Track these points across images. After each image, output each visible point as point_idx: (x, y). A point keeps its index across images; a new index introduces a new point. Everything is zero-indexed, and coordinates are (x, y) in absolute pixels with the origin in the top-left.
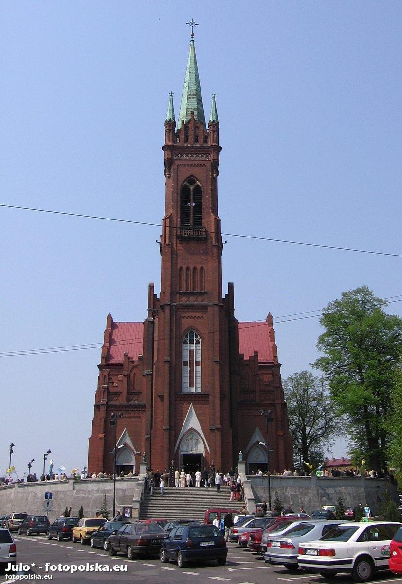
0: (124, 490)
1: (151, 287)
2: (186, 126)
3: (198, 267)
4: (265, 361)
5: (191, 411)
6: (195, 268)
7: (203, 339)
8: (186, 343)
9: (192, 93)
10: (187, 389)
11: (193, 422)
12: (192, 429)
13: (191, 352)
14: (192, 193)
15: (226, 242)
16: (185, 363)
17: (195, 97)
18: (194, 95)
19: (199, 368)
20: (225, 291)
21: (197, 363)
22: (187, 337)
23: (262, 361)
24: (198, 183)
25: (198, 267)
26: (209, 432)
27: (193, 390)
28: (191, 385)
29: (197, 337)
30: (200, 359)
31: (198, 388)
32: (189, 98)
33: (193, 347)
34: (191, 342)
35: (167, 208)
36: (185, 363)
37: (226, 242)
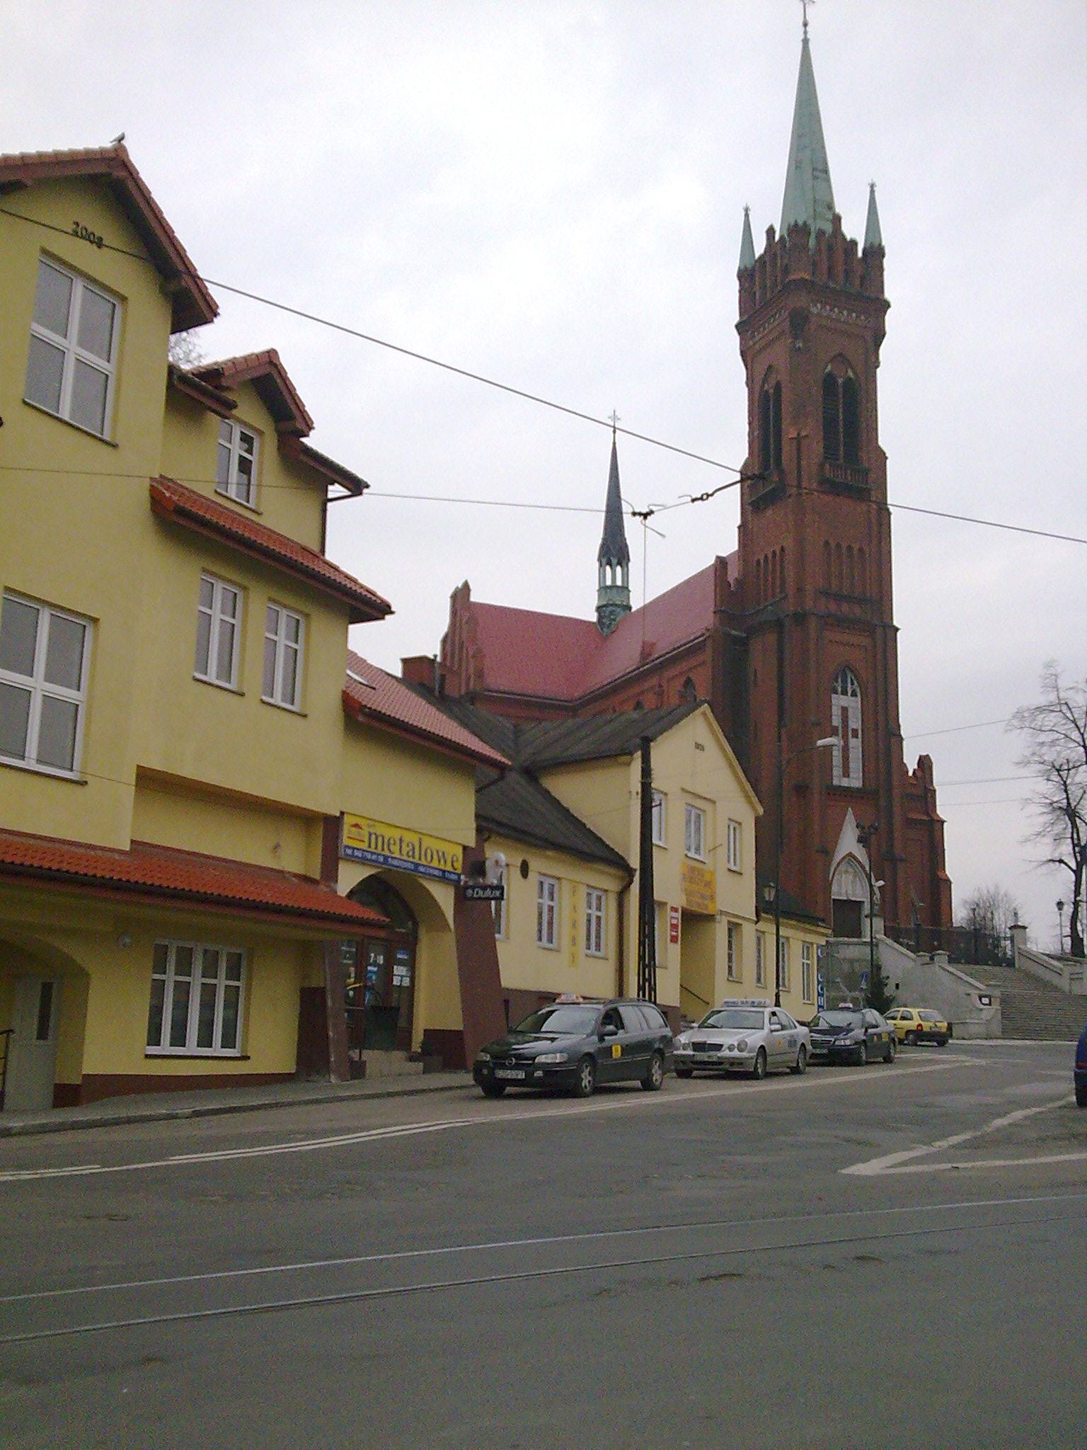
0: (852, 961)
3: (856, 547)
4: (552, 696)
6: (850, 548)
8: (836, 693)
10: (839, 780)
11: (848, 842)
13: (845, 710)
14: (841, 390)
19: (855, 744)
21: (855, 732)
23: (492, 687)
24: (850, 374)
25: (856, 547)
27: (845, 782)
28: (846, 773)
29: (852, 684)
31: (855, 781)
34: (844, 693)
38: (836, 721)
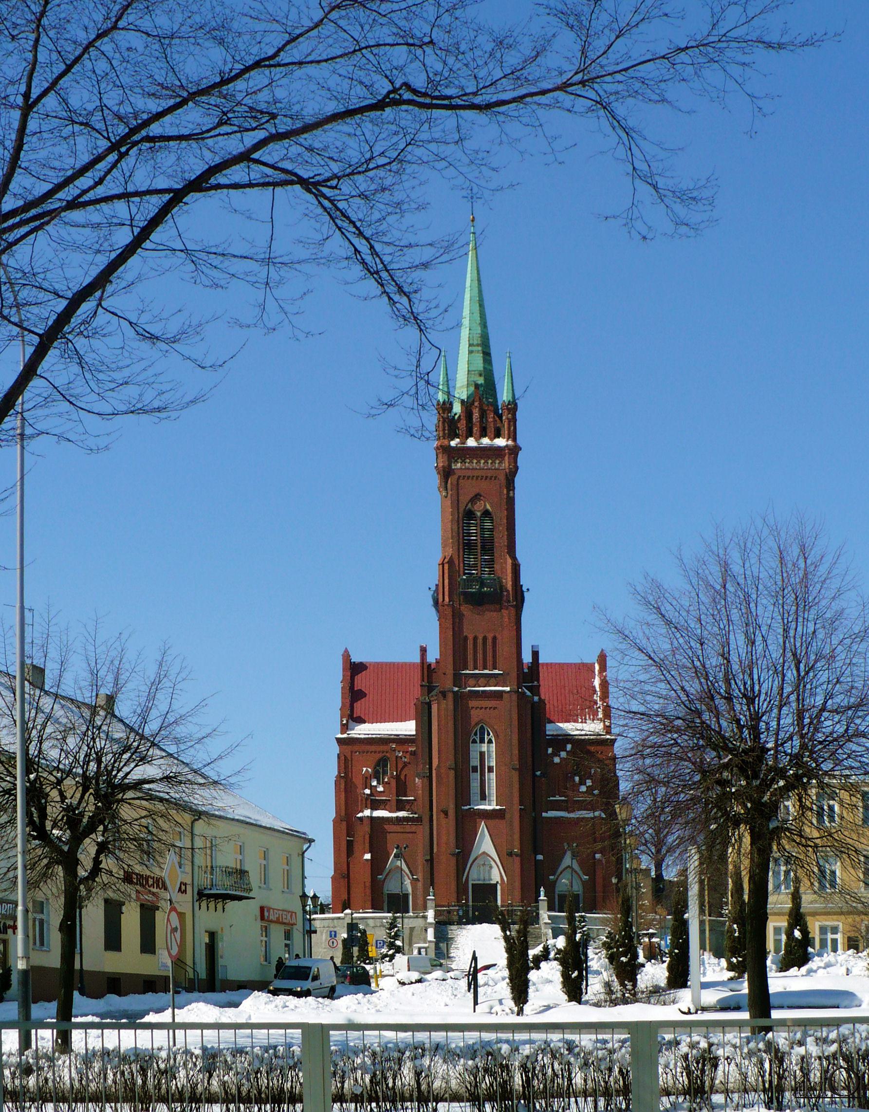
1: (423, 650)
2: (467, 405)
3: (490, 636)
5: (483, 830)
7: (497, 736)
8: (474, 742)
9: (475, 342)
11: (485, 844)
12: (484, 853)
15: (528, 590)
16: (475, 769)
17: (480, 348)
18: (478, 345)
19: (493, 776)
20: (527, 658)
22: (476, 734)
25: (490, 636)
26: (505, 856)
30: (493, 763)
32: (470, 352)
33: (484, 747)
34: (482, 741)
35: (444, 546)
36: (475, 769)
37: (528, 590)
38: (475, 762)
